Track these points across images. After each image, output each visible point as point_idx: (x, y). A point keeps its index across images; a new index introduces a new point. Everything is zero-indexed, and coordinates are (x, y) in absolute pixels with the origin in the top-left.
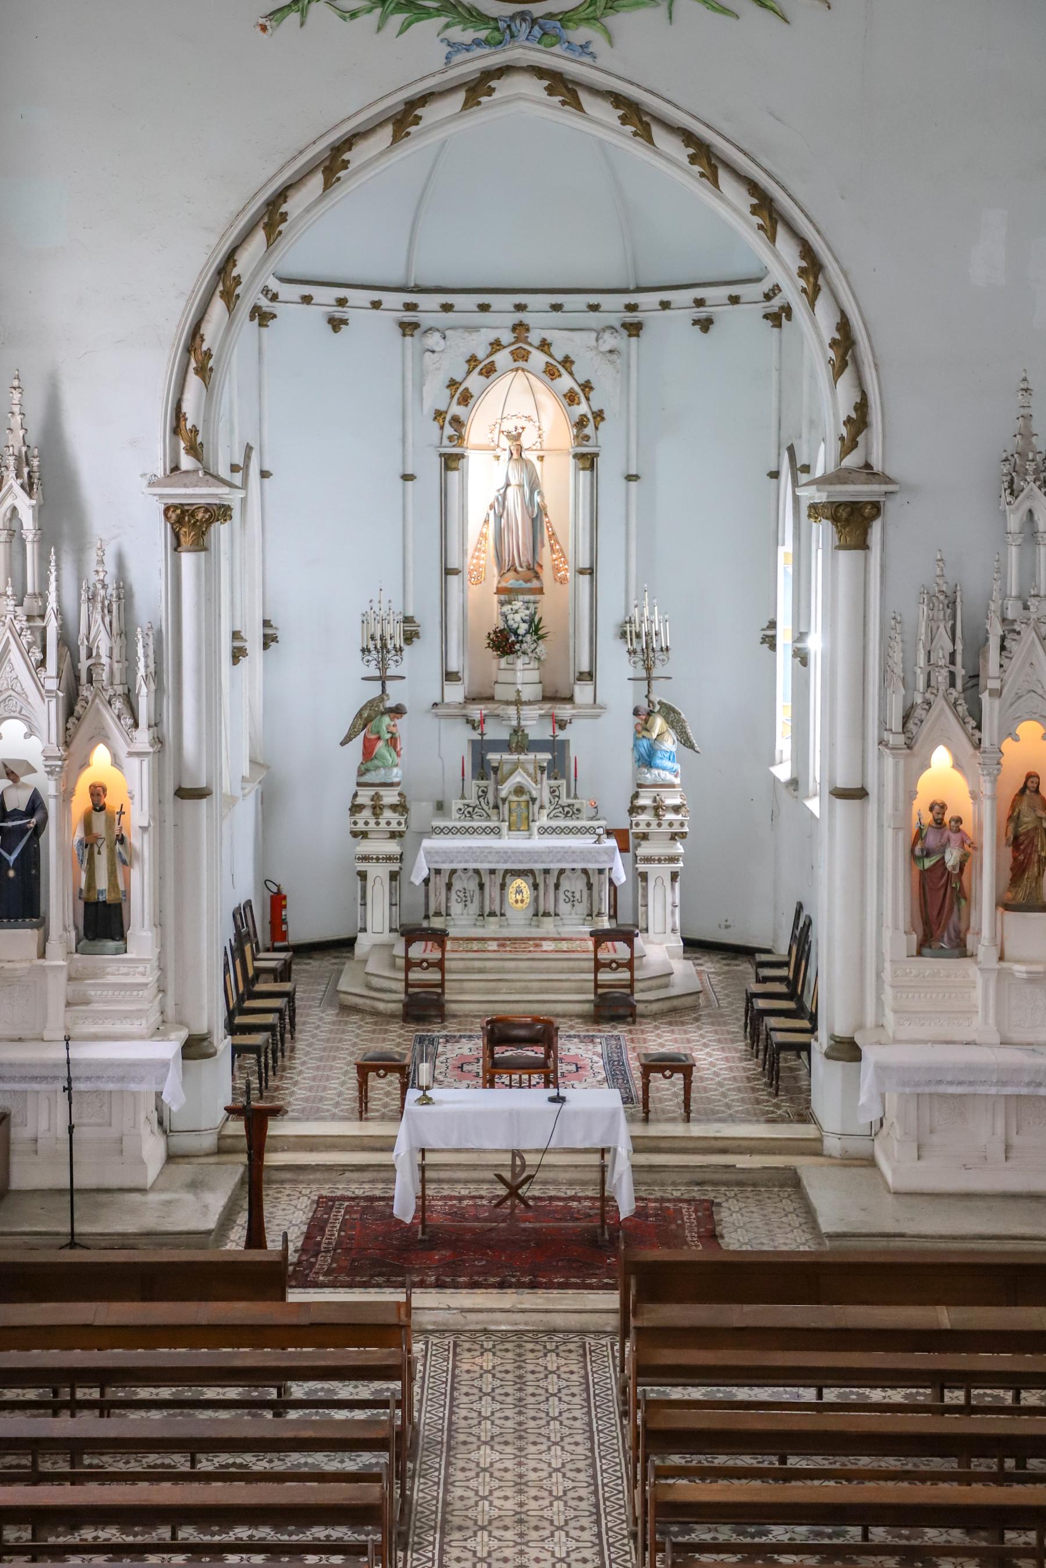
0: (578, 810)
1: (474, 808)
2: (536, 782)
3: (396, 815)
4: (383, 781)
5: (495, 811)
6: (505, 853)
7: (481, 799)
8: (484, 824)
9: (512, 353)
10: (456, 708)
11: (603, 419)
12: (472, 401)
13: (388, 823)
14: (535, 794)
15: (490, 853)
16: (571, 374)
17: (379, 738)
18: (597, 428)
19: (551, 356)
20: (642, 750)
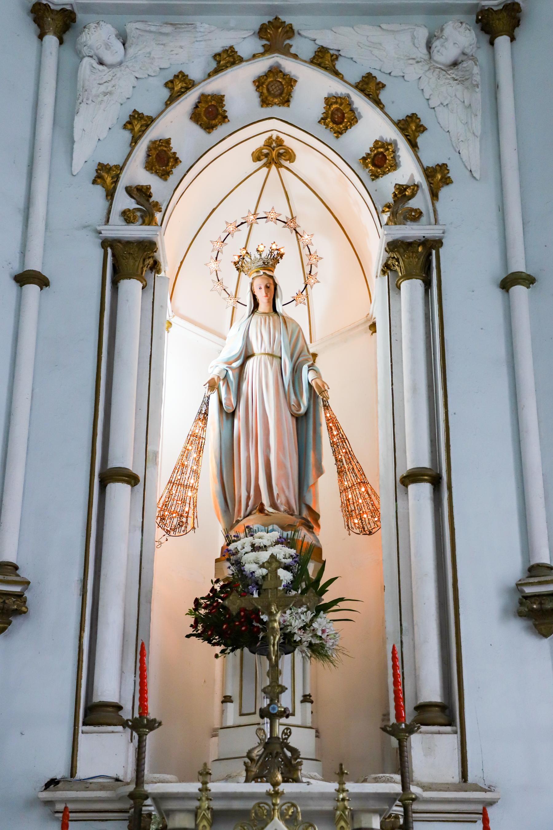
9: (259, 83)
11: (447, 181)
12: (178, 171)
16: (378, 103)
18: (434, 195)
19: (337, 74)
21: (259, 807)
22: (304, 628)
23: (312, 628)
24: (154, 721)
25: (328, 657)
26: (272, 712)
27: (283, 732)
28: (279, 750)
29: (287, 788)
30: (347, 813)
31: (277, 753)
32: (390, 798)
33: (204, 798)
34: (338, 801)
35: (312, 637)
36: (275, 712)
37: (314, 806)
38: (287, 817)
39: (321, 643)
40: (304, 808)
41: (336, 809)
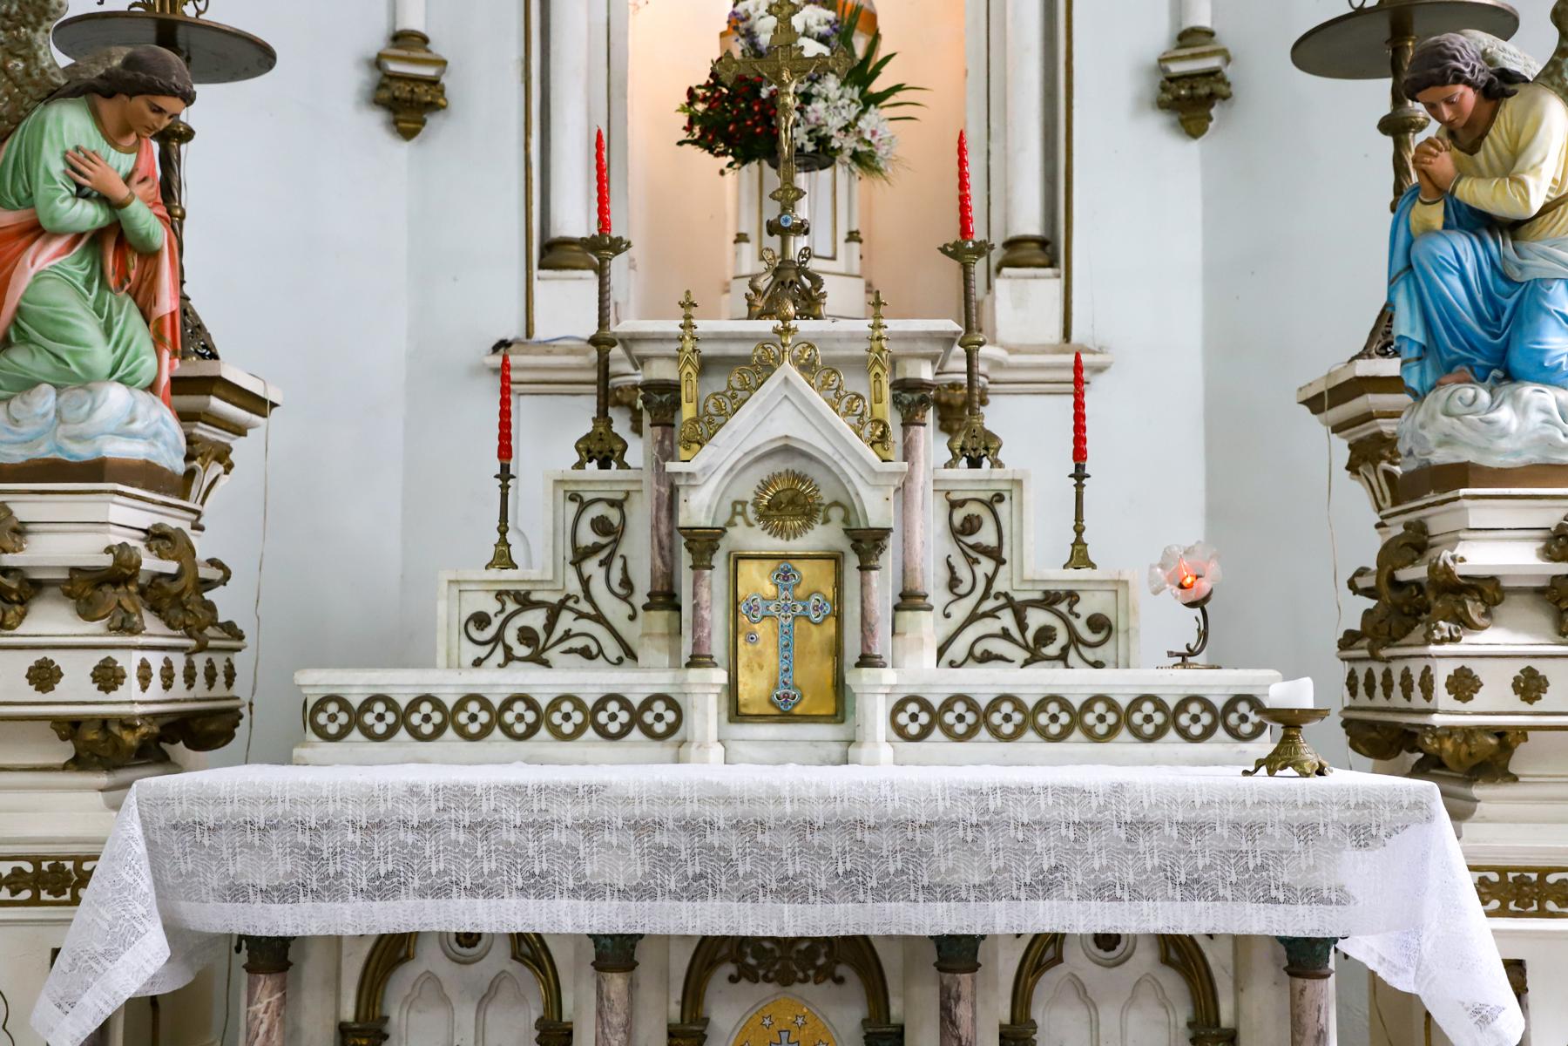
0: (1099, 623)
1: (554, 612)
2: (881, 441)
3: (93, 630)
4: (44, 451)
5: (659, 618)
6: (690, 826)
7: (592, 567)
8: (591, 681)
10: (571, 352)
13: (44, 676)
14: (876, 510)
15: (590, 828)
17: (35, 231)
20: (1453, 288)
21: (763, 348)
22: (846, 129)
23: (857, 129)
24: (620, 239)
25: (879, 170)
26: (784, 225)
27: (800, 254)
28: (794, 278)
29: (805, 326)
30: (884, 356)
31: (792, 282)
32: (948, 340)
33: (687, 338)
34: (872, 340)
35: (857, 141)
36: (788, 225)
37: (841, 351)
38: (802, 361)
39: (870, 151)
40: (825, 353)
41: (871, 350)
